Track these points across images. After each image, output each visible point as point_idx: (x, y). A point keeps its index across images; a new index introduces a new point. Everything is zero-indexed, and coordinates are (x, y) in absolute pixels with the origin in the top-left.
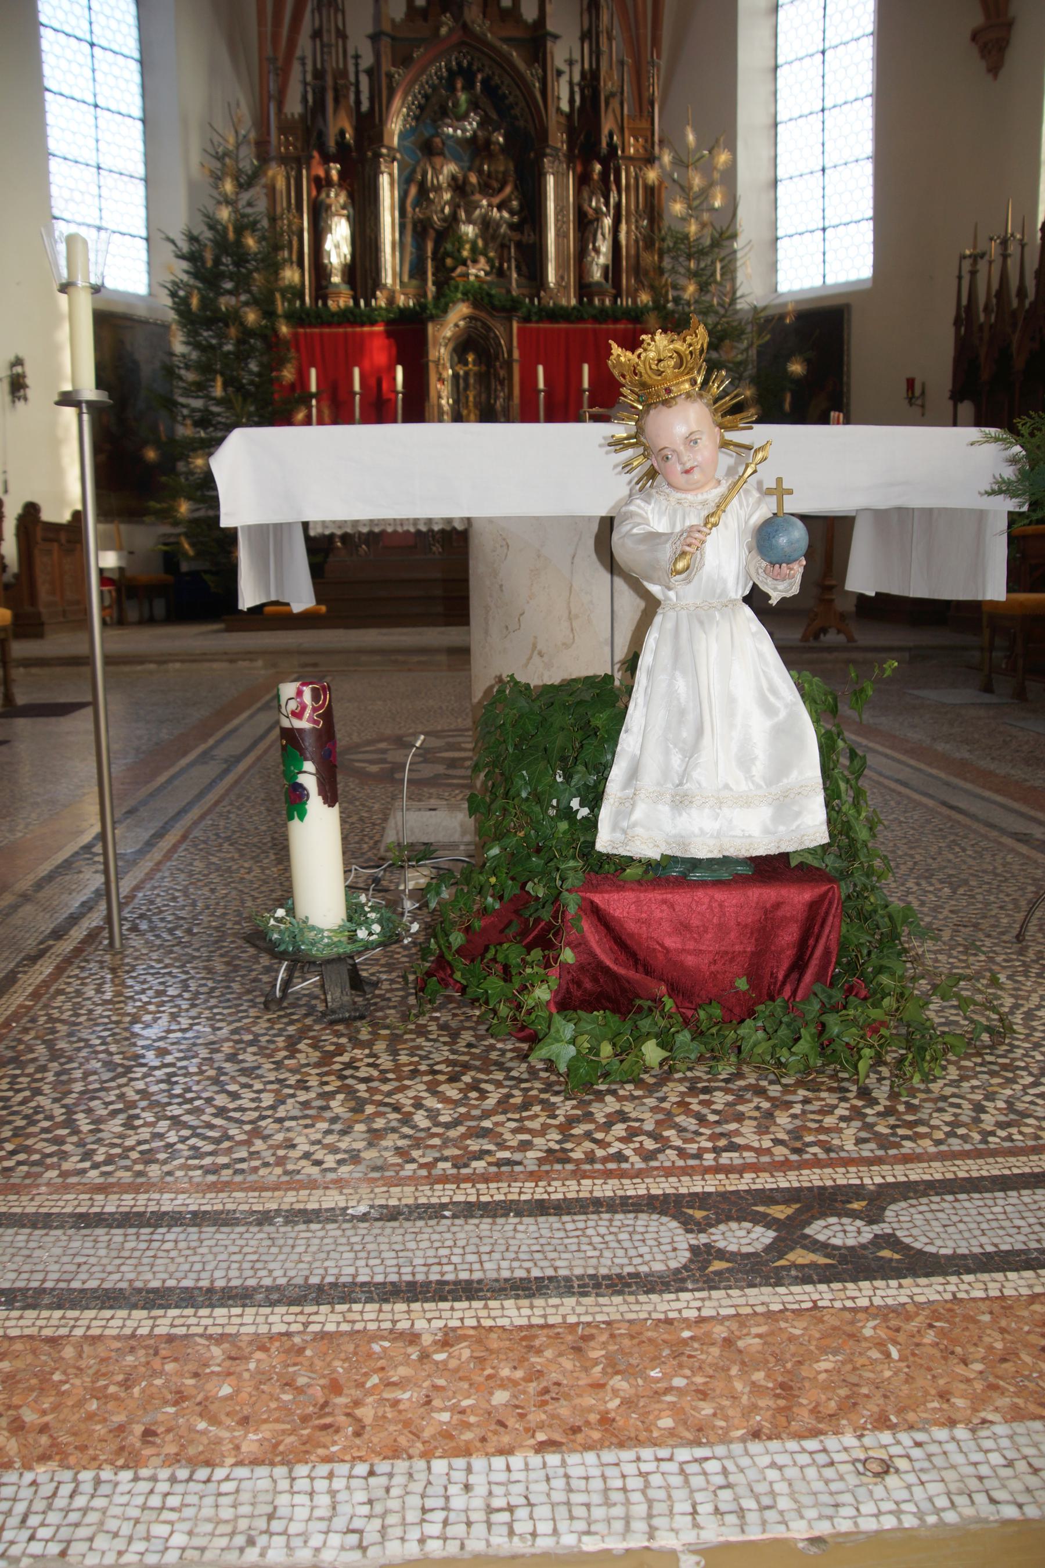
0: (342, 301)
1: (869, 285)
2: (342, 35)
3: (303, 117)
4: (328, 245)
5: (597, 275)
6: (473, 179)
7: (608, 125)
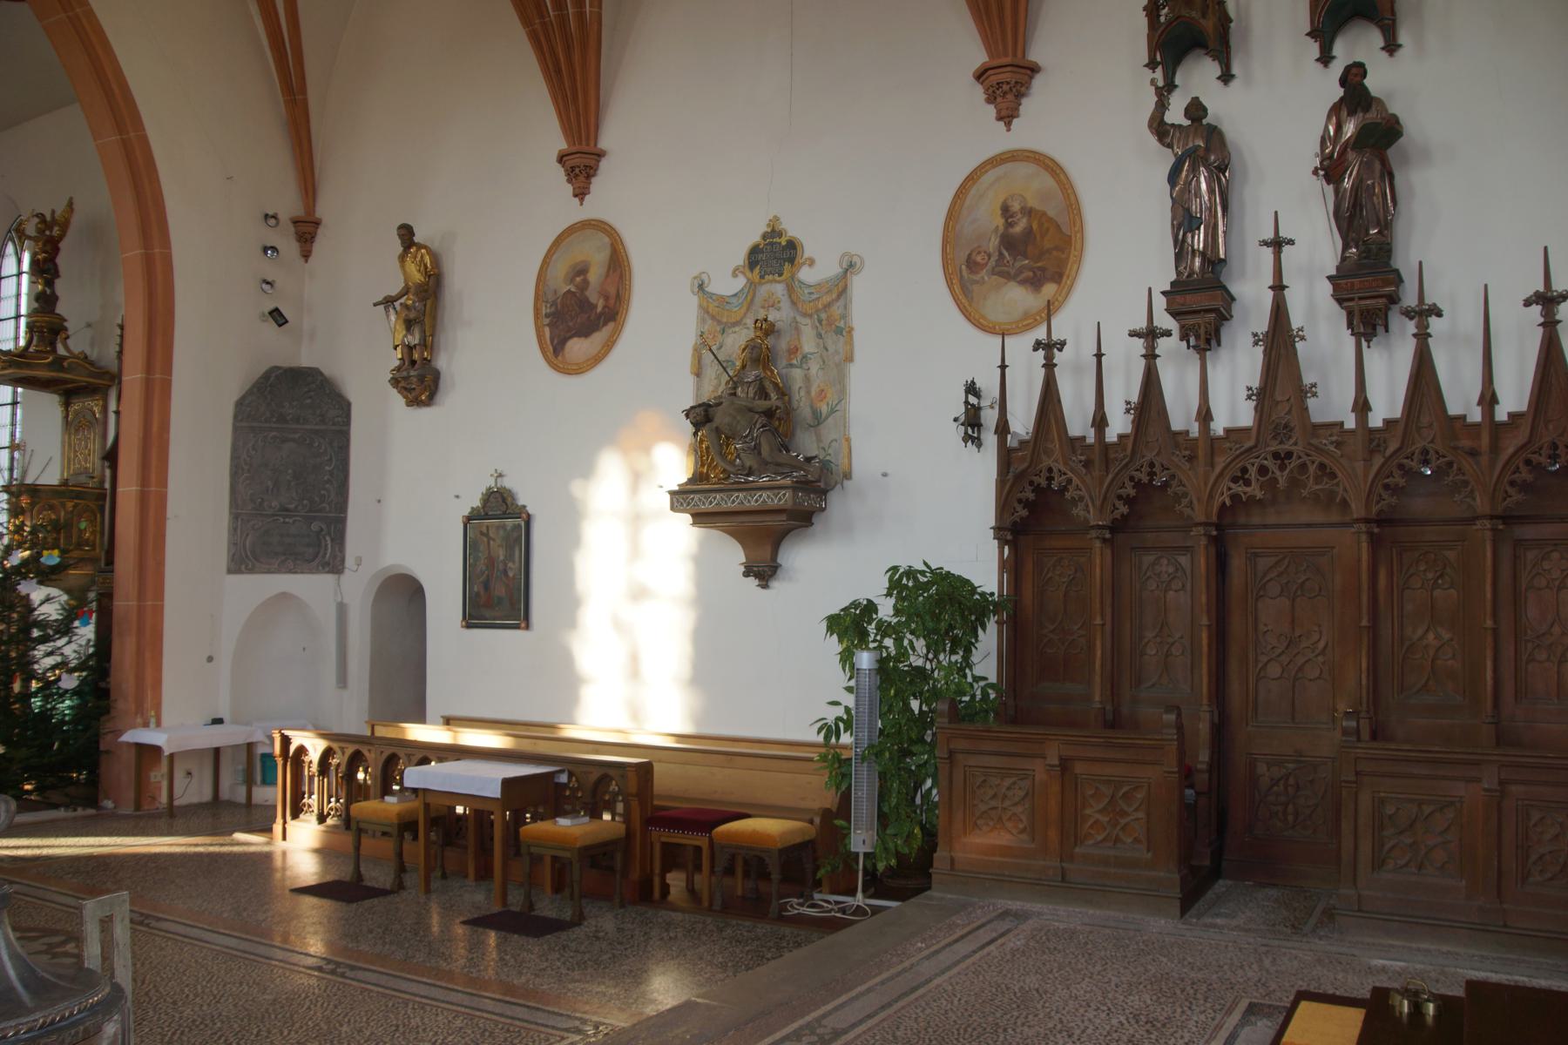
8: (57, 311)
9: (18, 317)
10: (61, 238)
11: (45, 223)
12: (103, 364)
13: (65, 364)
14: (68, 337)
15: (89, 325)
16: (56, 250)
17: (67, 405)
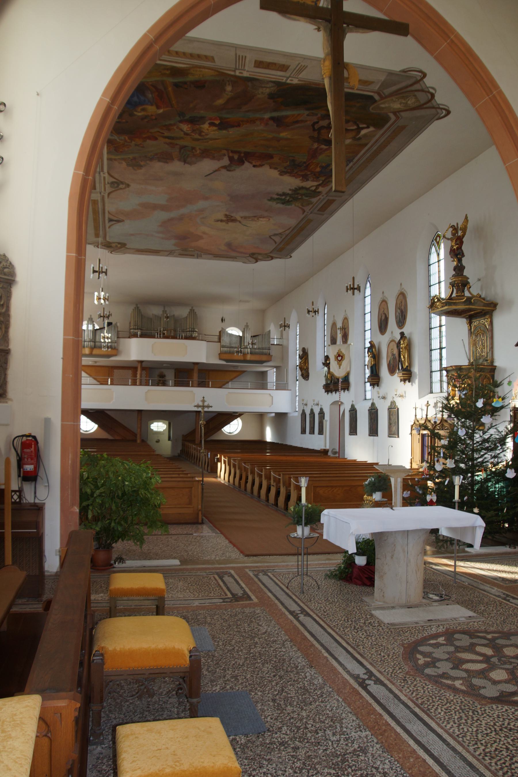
8: (464, 274)
9: (439, 282)
10: (463, 236)
11: (455, 229)
12: (488, 299)
13: (472, 301)
14: (470, 288)
15: (479, 280)
16: (462, 243)
17: (470, 323)
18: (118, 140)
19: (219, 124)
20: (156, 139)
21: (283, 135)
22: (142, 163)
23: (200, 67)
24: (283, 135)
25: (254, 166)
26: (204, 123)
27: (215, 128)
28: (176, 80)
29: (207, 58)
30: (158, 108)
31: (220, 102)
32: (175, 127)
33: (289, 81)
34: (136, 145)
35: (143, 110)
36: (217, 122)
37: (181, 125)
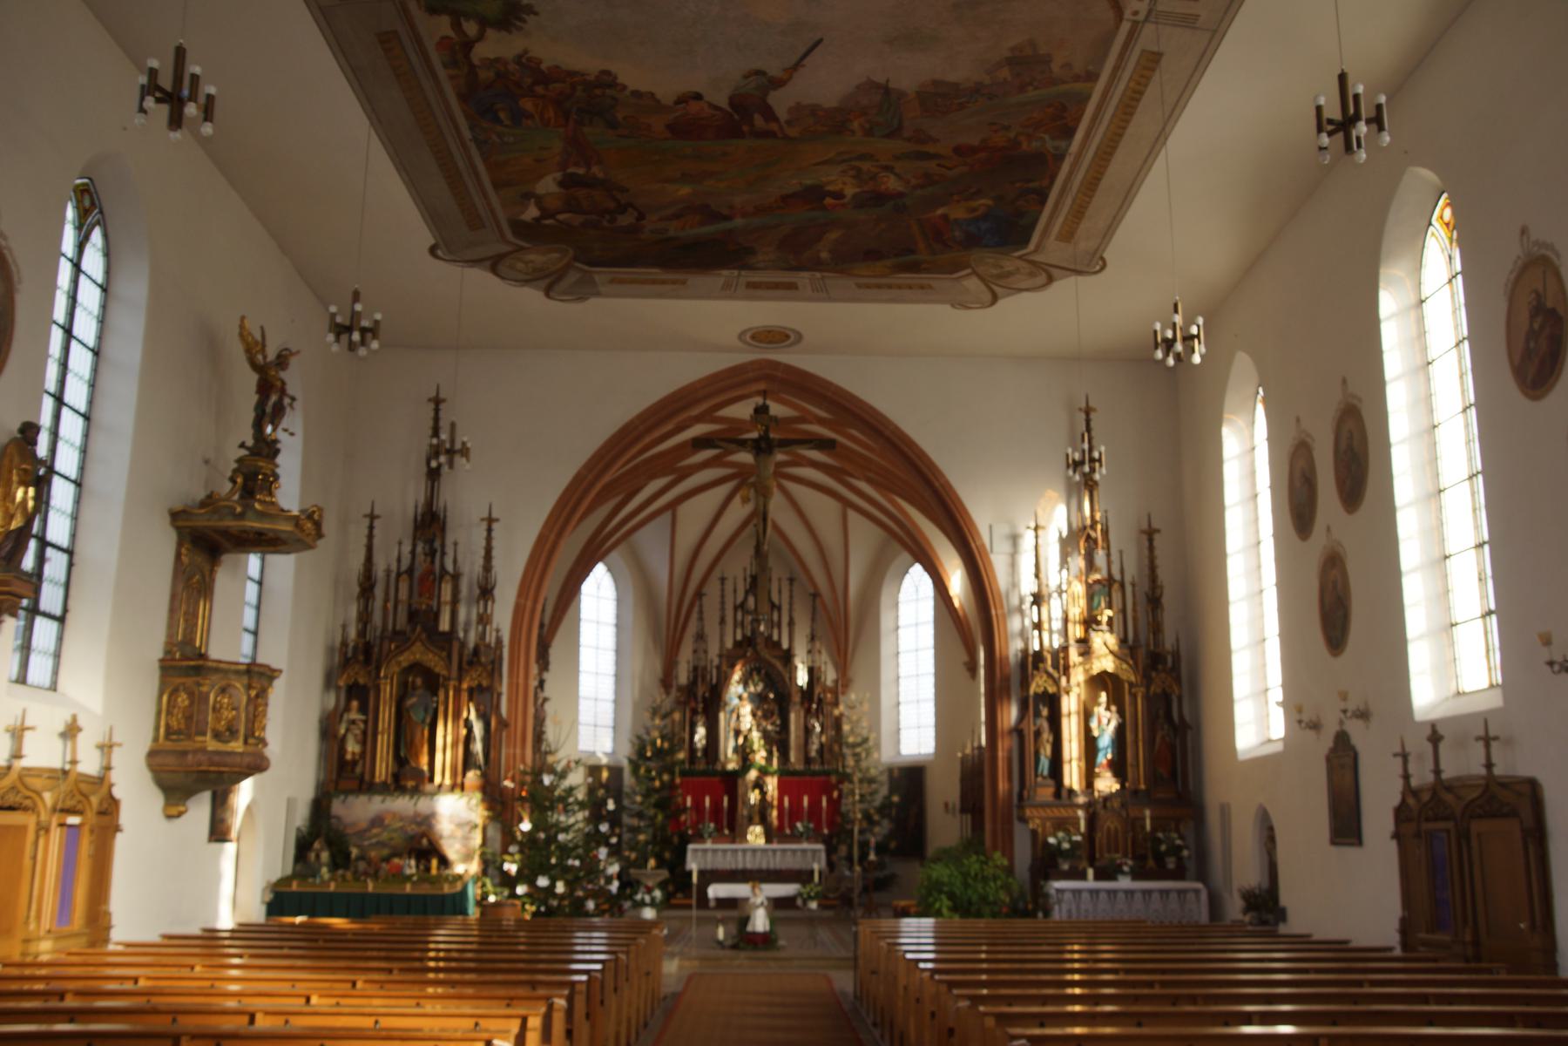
0: (701, 766)
1: (932, 758)
2: (706, 652)
3: (688, 686)
4: (697, 738)
5: (813, 754)
6: (759, 713)
7: (817, 690)
18: (1047, 137)
19: (824, 199)
20: (959, 150)
21: (685, 190)
22: (1005, 73)
23: (874, 277)
24: (685, 190)
25: (698, 97)
26: (855, 196)
27: (830, 188)
28: (911, 258)
29: (868, 286)
30: (945, 217)
31: (833, 235)
32: (914, 182)
33: (736, 273)
34: (1007, 128)
35: (974, 210)
36: (828, 201)
37: (900, 189)
